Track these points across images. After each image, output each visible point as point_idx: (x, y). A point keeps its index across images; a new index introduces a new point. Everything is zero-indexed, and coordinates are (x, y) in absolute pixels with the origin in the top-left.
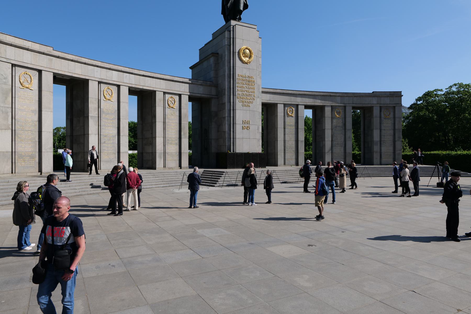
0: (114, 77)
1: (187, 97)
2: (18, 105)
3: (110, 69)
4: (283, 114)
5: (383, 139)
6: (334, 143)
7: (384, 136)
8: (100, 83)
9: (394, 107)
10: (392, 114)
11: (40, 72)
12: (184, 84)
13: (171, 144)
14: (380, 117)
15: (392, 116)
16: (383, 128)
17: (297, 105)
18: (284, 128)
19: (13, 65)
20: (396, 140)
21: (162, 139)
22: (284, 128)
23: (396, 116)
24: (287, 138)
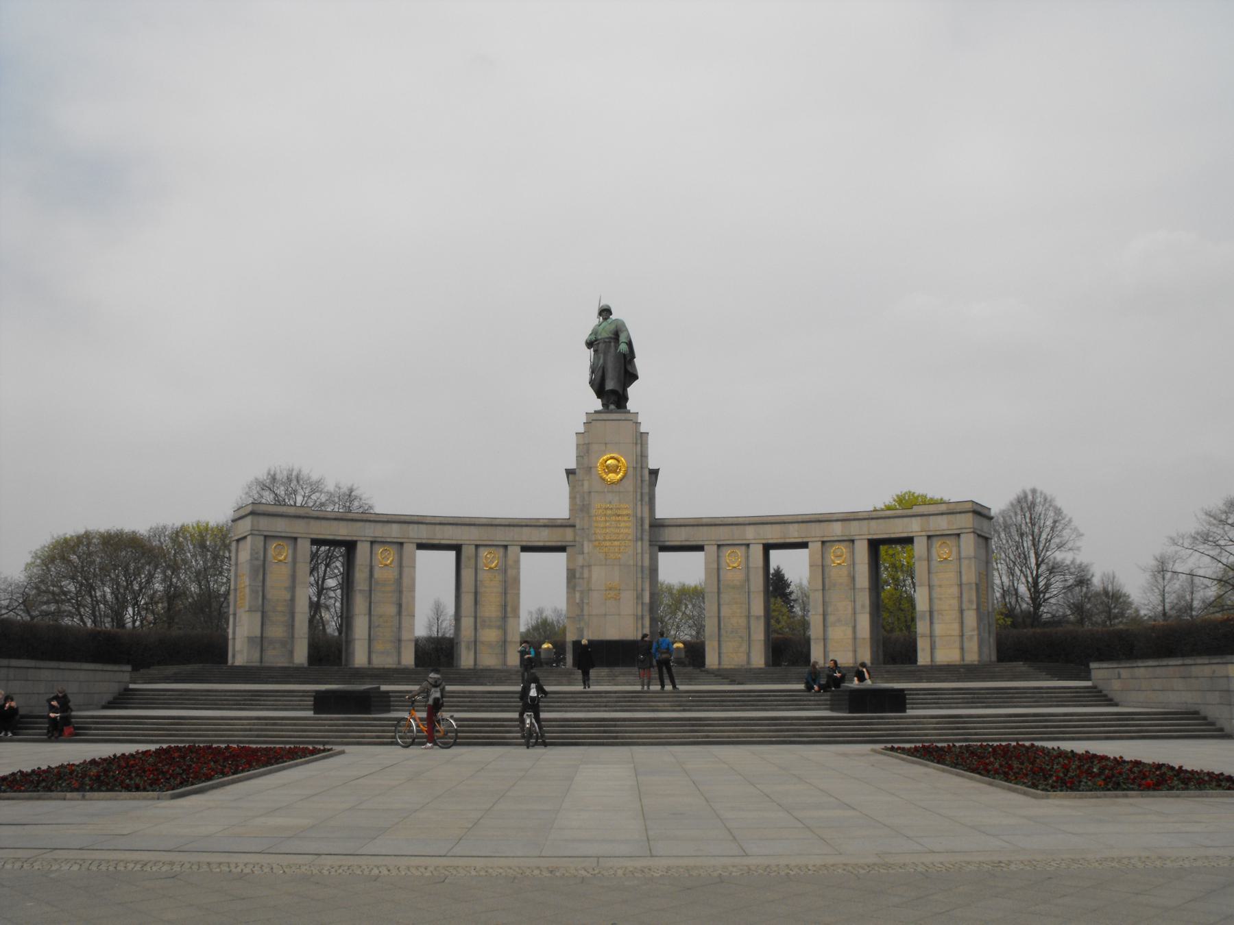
0: (394, 532)
1: (519, 549)
2: (268, 583)
3: (388, 522)
4: (715, 566)
5: (936, 607)
6: (831, 619)
7: (940, 599)
8: (372, 543)
9: (958, 535)
10: (955, 550)
11: (295, 539)
13: (490, 627)
14: (929, 560)
15: (954, 555)
16: (935, 581)
17: (748, 545)
18: (719, 593)
19: (266, 537)
20: (964, 607)
21: (472, 620)
22: (719, 593)
23: (963, 555)
24: (725, 611)
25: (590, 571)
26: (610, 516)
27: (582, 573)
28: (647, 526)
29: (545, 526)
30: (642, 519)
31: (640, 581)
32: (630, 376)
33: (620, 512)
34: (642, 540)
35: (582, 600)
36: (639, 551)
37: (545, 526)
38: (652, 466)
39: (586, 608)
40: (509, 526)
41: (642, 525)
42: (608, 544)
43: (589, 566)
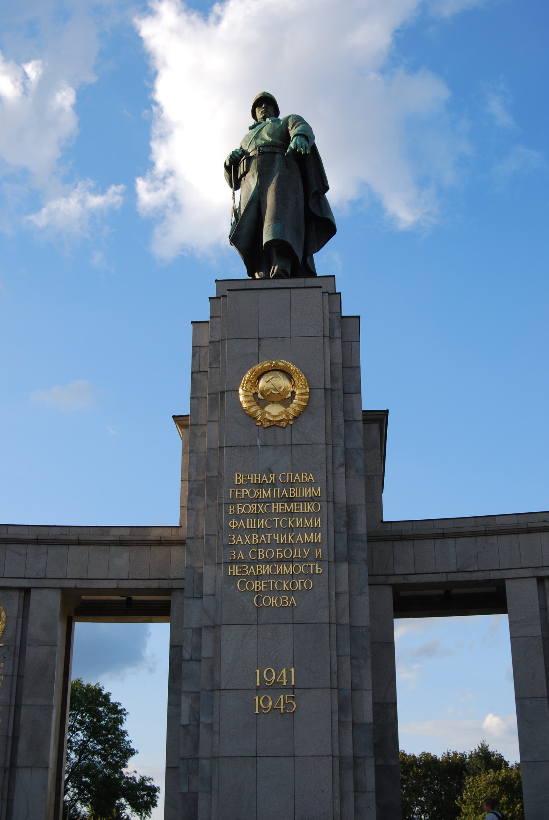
12: (44, 548)
25: (217, 640)
26: (268, 501)
27: (197, 648)
28: (362, 529)
29: (121, 543)
30: (350, 511)
31: (347, 663)
32: (321, 227)
33: (295, 493)
34: (349, 560)
35: (195, 716)
36: (344, 587)
37: (121, 543)
38: (369, 402)
39: (203, 730)
40: (38, 542)
41: (350, 523)
42: (266, 569)
43: (216, 626)
